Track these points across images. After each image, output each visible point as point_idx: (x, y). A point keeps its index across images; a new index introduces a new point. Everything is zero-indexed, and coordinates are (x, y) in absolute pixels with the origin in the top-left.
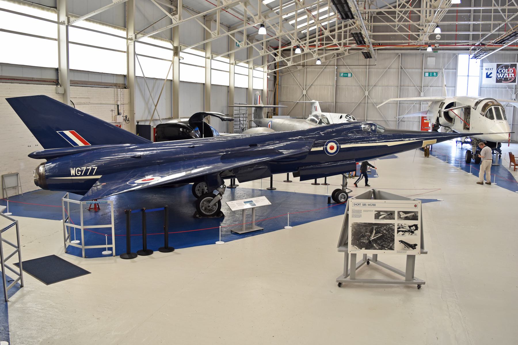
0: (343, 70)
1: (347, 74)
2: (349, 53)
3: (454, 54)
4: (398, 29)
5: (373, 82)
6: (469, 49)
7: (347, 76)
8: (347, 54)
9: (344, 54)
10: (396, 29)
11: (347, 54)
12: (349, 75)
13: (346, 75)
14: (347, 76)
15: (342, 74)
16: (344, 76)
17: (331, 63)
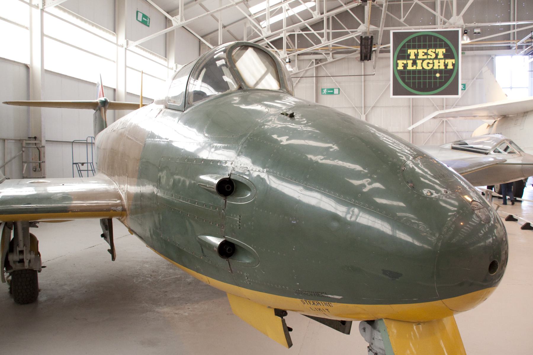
0: (326, 84)
1: (333, 89)
2: (333, 58)
3: (490, 56)
4: (405, 21)
5: (371, 102)
6: (509, 48)
7: (333, 93)
8: (330, 59)
9: (326, 60)
10: (402, 20)
11: (330, 59)
12: (336, 91)
13: (331, 92)
14: (333, 93)
15: (325, 91)
16: (328, 94)
17: (308, 74)
